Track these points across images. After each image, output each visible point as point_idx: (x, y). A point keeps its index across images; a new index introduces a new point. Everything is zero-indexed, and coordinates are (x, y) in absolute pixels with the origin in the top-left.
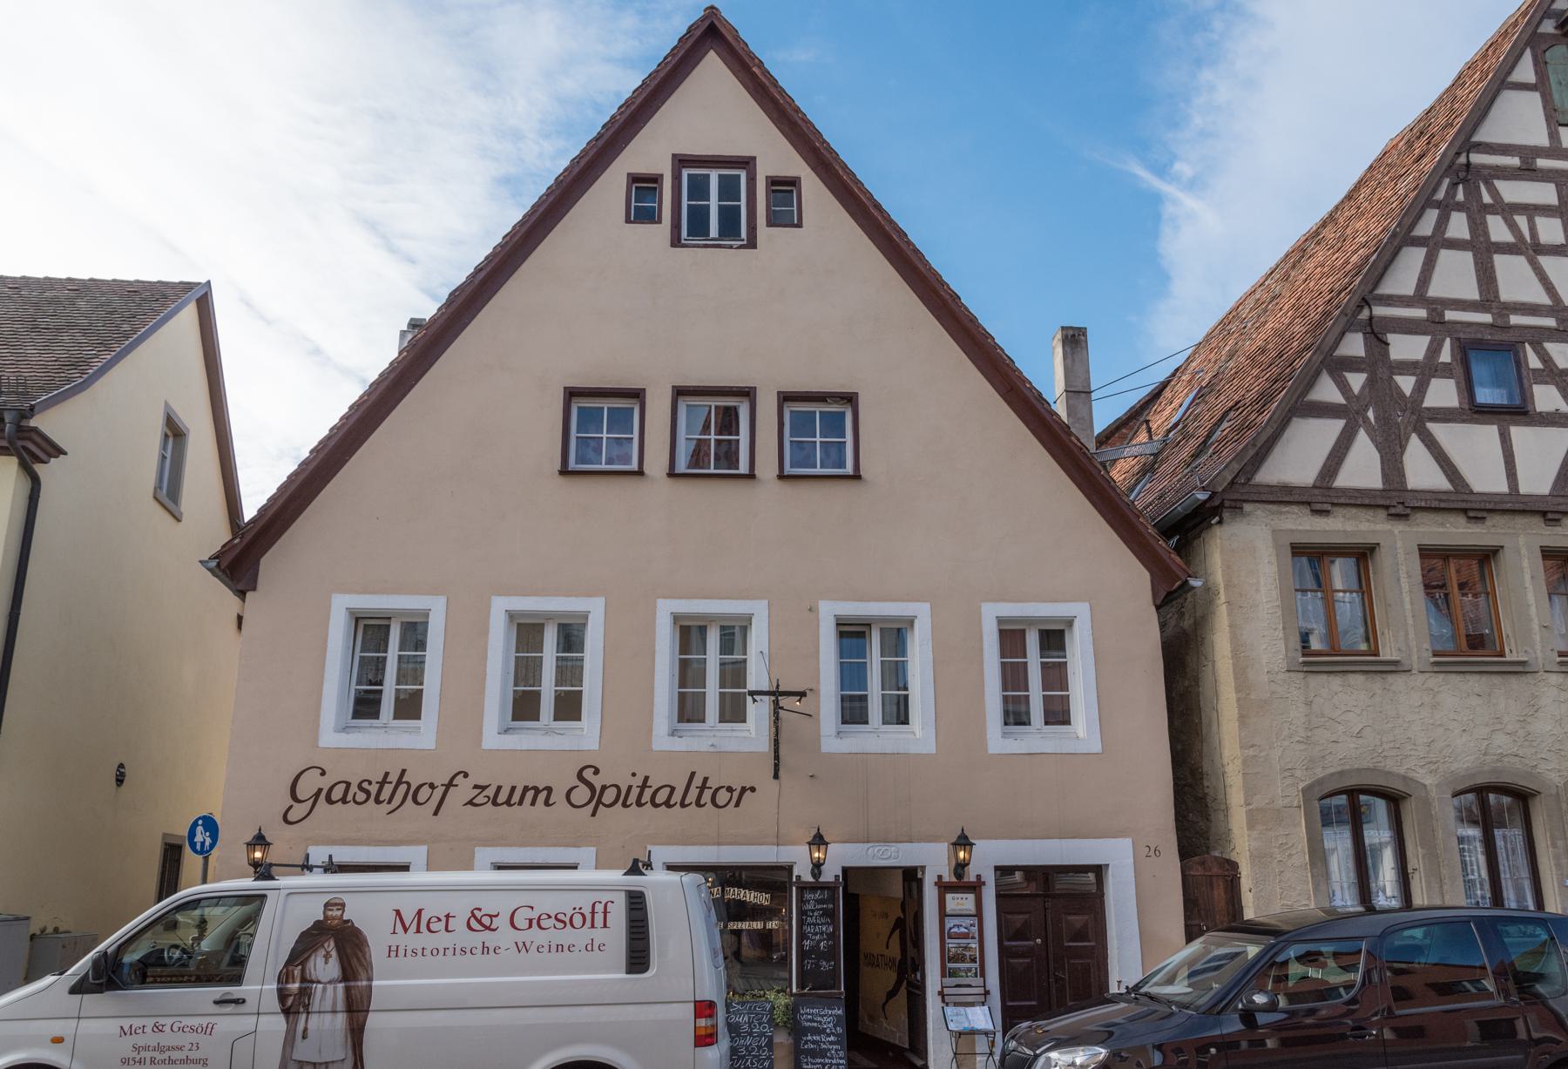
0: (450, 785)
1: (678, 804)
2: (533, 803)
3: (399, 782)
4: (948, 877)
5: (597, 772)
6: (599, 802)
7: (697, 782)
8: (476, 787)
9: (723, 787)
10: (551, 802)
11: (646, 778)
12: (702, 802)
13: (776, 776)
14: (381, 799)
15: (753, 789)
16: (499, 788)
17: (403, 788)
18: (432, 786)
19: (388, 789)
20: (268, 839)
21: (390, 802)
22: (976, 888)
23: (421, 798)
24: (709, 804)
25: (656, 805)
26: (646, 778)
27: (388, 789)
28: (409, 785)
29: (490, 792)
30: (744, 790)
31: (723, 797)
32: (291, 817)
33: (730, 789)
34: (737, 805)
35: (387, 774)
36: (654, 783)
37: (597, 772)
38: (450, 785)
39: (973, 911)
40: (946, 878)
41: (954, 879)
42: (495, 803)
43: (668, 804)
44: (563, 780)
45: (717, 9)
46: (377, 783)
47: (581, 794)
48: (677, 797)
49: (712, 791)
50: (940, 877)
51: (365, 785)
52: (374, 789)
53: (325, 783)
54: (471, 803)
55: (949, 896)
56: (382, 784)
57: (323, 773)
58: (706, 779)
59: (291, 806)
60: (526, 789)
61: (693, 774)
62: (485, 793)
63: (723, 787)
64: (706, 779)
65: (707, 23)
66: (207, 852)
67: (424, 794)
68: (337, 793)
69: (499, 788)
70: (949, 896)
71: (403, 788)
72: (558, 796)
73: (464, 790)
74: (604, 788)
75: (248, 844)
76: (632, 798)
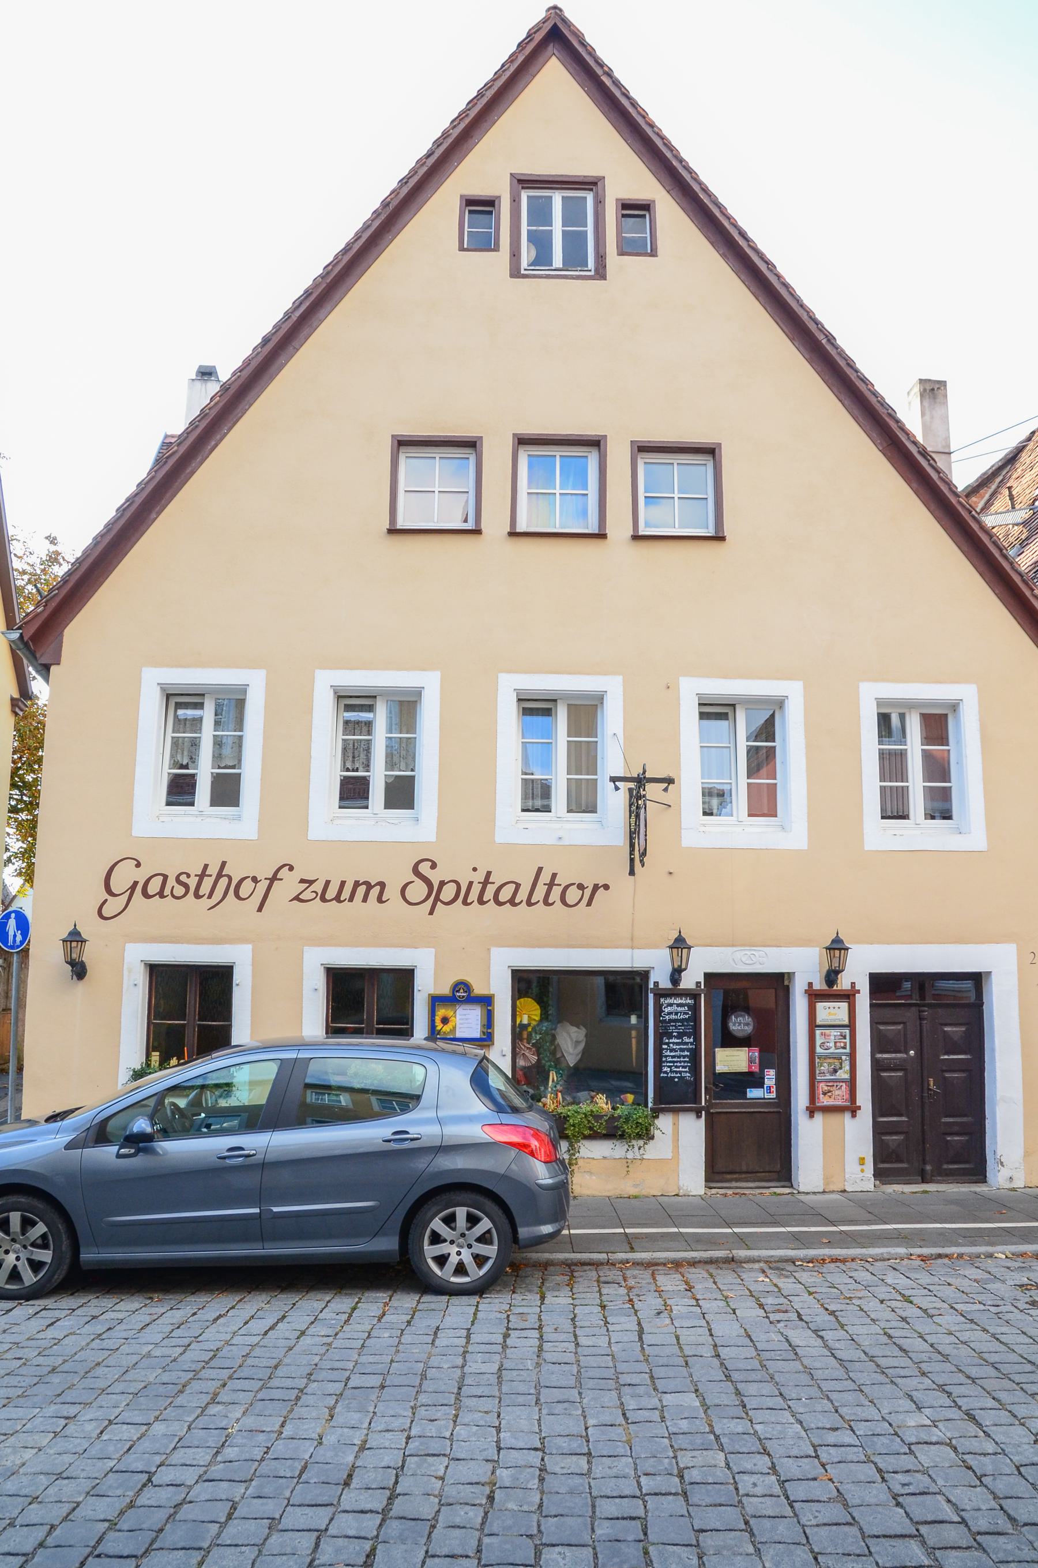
0: (274, 879)
1: (524, 902)
2: (365, 900)
3: (220, 875)
4: (819, 985)
5: (434, 866)
6: (437, 899)
7: (545, 878)
8: (302, 881)
9: (574, 884)
10: (384, 899)
11: (489, 874)
12: (550, 901)
14: (201, 893)
15: (606, 887)
16: (328, 883)
17: (224, 881)
18: (255, 880)
19: (207, 883)
20: (84, 936)
21: (210, 897)
22: (849, 996)
23: (243, 893)
24: (558, 903)
25: (500, 904)
26: (489, 874)
27: (207, 883)
28: (230, 878)
29: (318, 887)
30: (596, 888)
31: (573, 894)
32: (106, 912)
33: (581, 887)
34: (589, 904)
35: (206, 866)
36: (497, 879)
37: (434, 866)
38: (274, 879)
39: (846, 1022)
40: (817, 986)
41: (825, 987)
42: (323, 899)
43: (512, 902)
44: (397, 875)
45: (561, 10)
46: (196, 875)
47: (418, 890)
48: (523, 895)
49: (561, 888)
50: (810, 984)
51: (183, 878)
52: (192, 882)
53: (141, 875)
54: (297, 898)
56: (202, 876)
57: (138, 865)
58: (554, 876)
59: (106, 900)
60: (357, 884)
61: (540, 869)
62: (312, 888)
63: (574, 884)
64: (554, 876)
65: (548, 26)
68: (154, 887)
69: (328, 883)
70: (820, 1006)
71: (224, 881)
72: (392, 892)
73: (288, 886)
74: (442, 884)
75: (64, 941)
76: (474, 896)
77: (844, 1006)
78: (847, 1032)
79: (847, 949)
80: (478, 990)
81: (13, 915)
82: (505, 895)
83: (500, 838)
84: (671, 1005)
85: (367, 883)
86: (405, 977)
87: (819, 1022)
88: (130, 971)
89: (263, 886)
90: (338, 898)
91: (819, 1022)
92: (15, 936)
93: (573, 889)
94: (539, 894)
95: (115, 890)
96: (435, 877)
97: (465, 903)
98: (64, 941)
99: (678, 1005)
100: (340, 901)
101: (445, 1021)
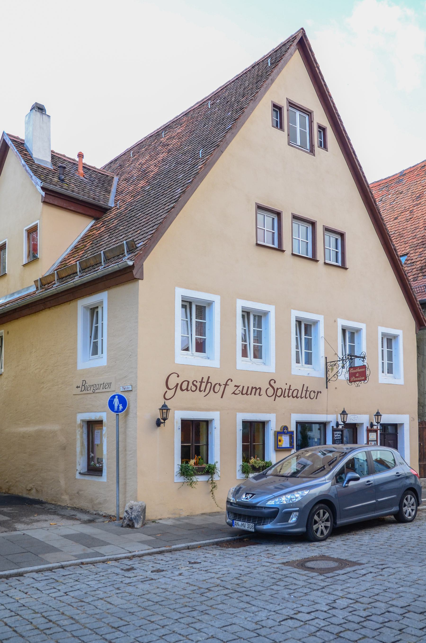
0: (226, 385)
3: (208, 382)
5: (275, 382)
6: (276, 395)
7: (305, 389)
8: (235, 386)
13: (327, 388)
14: (201, 390)
16: (243, 387)
18: (220, 385)
19: (204, 385)
21: (204, 391)
23: (216, 390)
24: (309, 397)
27: (204, 385)
29: (240, 389)
30: (318, 392)
31: (312, 395)
32: (167, 397)
33: (314, 392)
34: (316, 398)
35: (203, 378)
37: (275, 382)
38: (226, 385)
39: (375, 439)
42: (242, 394)
43: (297, 397)
44: (265, 386)
48: (299, 395)
50: (367, 427)
51: (195, 383)
52: (198, 385)
53: (180, 381)
55: (370, 434)
56: (201, 382)
57: (178, 376)
58: (307, 387)
59: (166, 392)
60: (252, 388)
64: (307, 387)
66: (120, 412)
67: (217, 387)
68: (184, 386)
69: (243, 387)
70: (370, 434)
71: (209, 385)
72: (263, 392)
73: (230, 388)
74: (278, 389)
75: (160, 409)
76: (286, 394)
77: (375, 434)
78: (376, 442)
79: (381, 415)
80: (289, 430)
81: (117, 397)
82: (295, 394)
83: (293, 373)
84: (336, 434)
85: (255, 388)
86: (263, 424)
87: (370, 439)
88: (177, 423)
89: (223, 387)
90: (246, 394)
91: (370, 439)
92: (118, 407)
93: (312, 392)
94: (303, 395)
95: (170, 387)
96: (276, 386)
97: (284, 397)
98: (160, 409)
99: (339, 434)
100: (247, 395)
101: (280, 441)
